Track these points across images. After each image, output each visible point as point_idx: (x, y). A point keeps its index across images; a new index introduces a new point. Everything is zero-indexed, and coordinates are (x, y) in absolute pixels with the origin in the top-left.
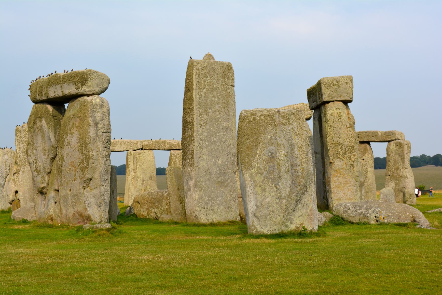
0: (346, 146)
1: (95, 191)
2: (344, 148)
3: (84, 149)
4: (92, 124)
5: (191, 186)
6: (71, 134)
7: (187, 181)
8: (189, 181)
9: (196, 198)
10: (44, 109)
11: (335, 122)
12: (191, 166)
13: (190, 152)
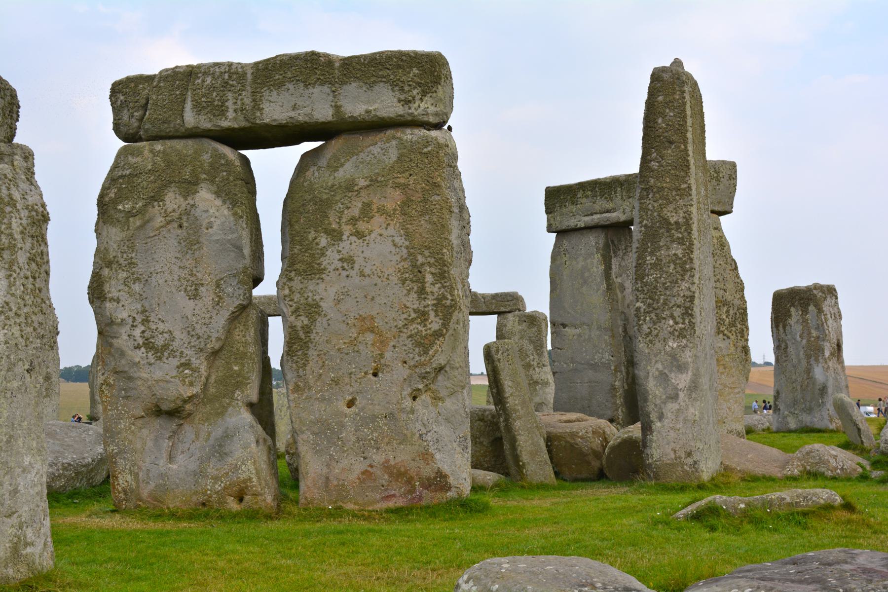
0: (736, 309)
1: (449, 404)
2: (731, 312)
3: (429, 278)
4: (456, 210)
5: (681, 386)
6: (360, 235)
7: (662, 373)
8: (672, 375)
9: (697, 418)
10: (206, 158)
11: (716, 257)
12: (681, 335)
13: (680, 301)
